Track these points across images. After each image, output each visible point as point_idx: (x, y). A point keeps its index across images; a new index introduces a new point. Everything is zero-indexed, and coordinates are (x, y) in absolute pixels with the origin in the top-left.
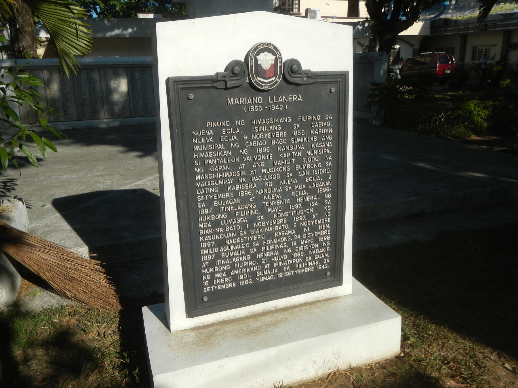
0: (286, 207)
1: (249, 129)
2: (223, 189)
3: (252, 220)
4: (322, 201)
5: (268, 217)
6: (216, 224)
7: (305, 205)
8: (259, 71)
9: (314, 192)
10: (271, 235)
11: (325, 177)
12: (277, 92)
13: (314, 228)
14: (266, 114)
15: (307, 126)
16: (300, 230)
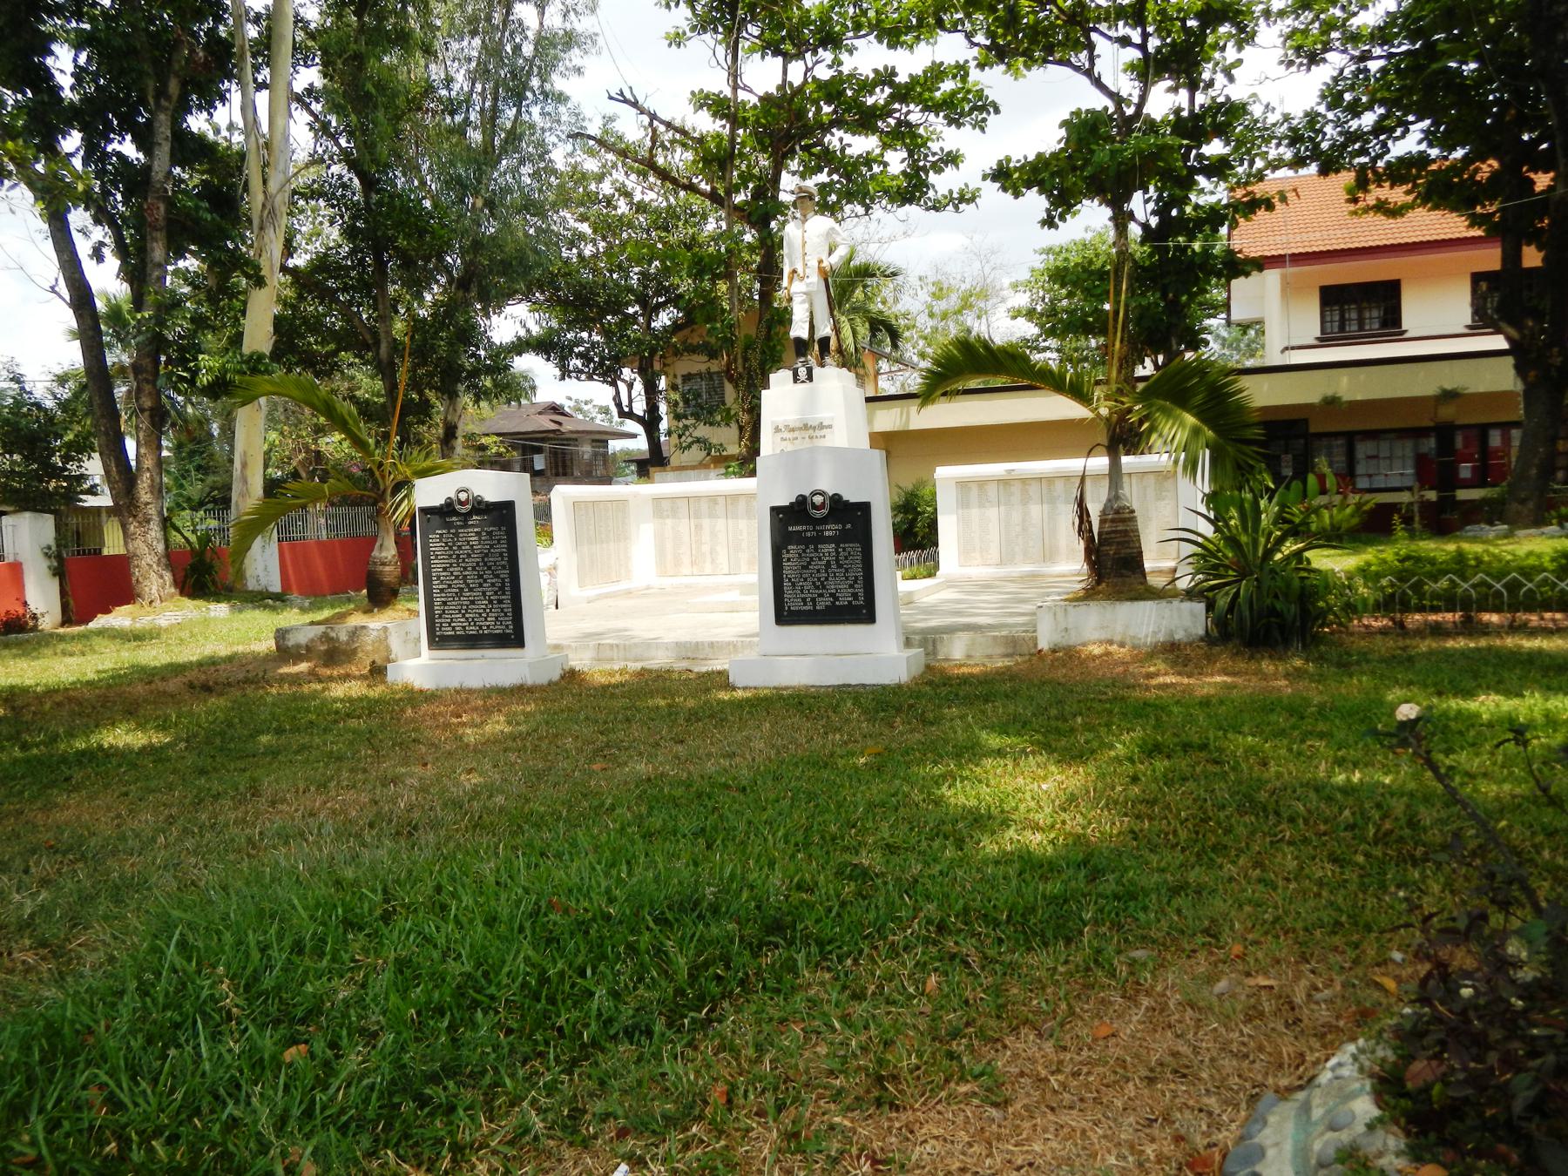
0: (481, 585)
1: (457, 535)
2: (445, 569)
3: (461, 590)
4: (503, 583)
5: (471, 590)
6: (442, 590)
7: (493, 585)
8: (461, 503)
9: (497, 576)
10: (473, 602)
11: (504, 567)
12: (469, 514)
13: (500, 602)
14: (466, 526)
15: (490, 534)
16: (491, 602)
